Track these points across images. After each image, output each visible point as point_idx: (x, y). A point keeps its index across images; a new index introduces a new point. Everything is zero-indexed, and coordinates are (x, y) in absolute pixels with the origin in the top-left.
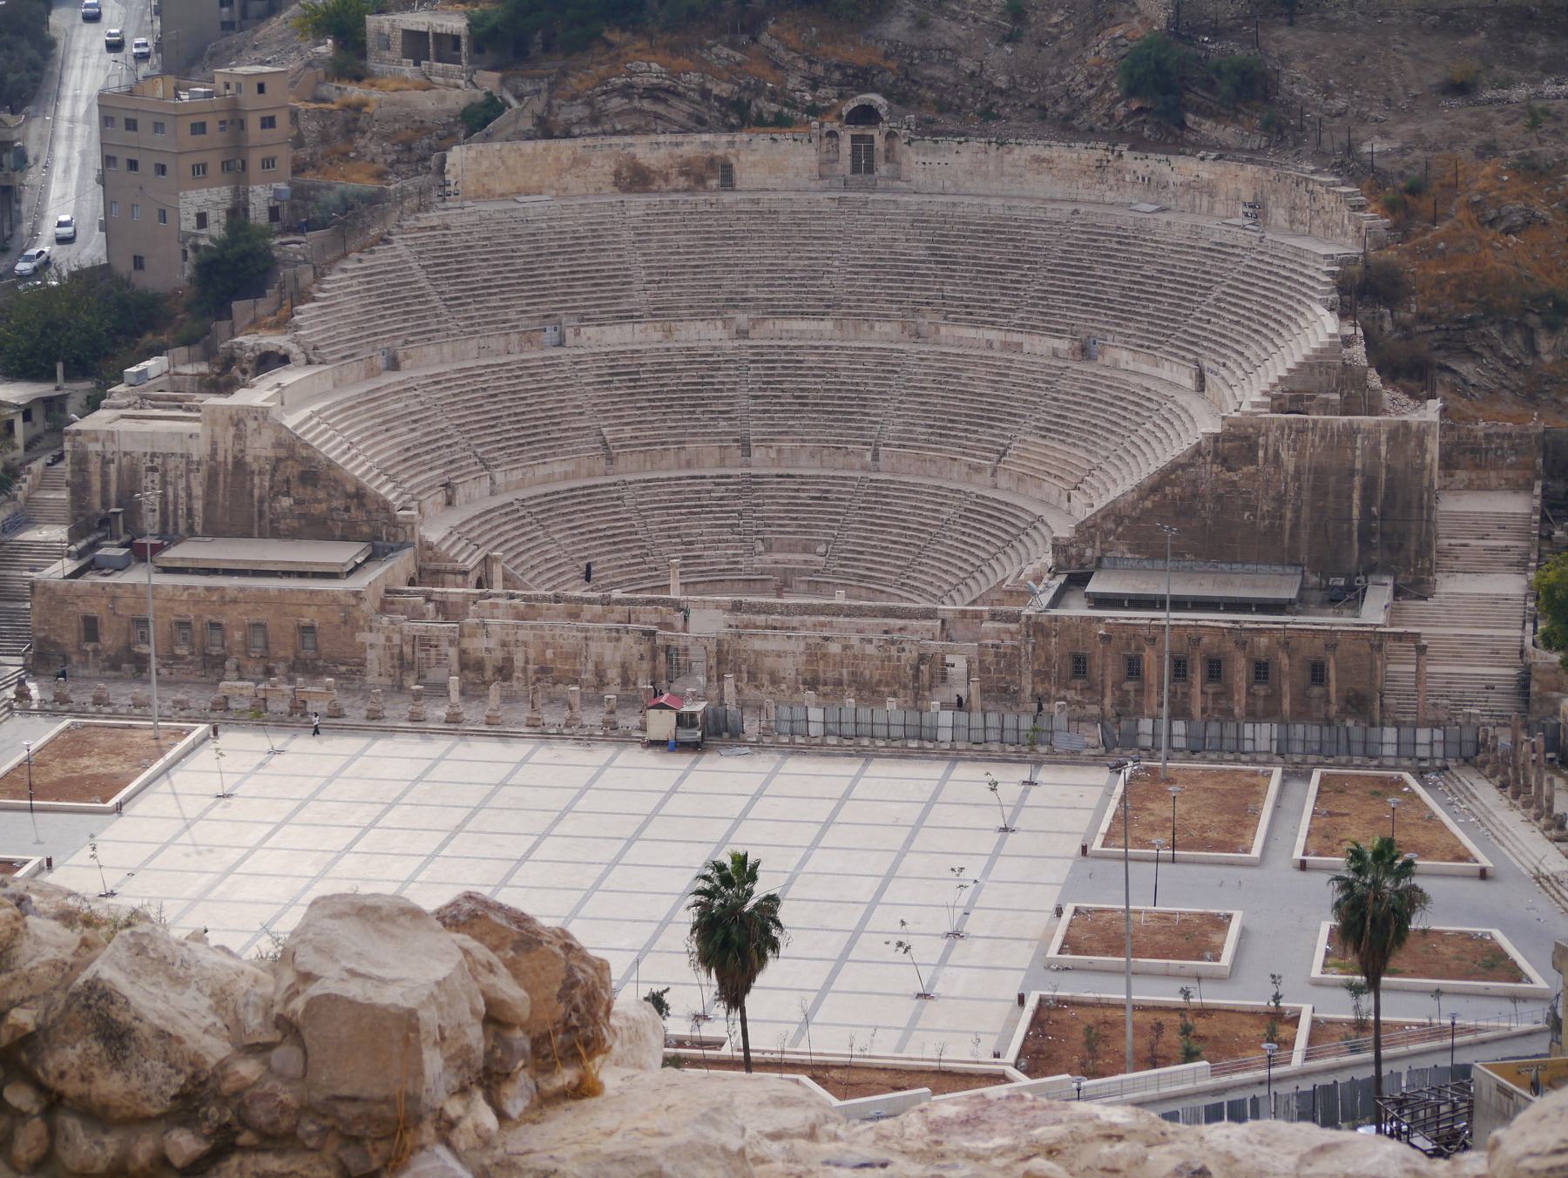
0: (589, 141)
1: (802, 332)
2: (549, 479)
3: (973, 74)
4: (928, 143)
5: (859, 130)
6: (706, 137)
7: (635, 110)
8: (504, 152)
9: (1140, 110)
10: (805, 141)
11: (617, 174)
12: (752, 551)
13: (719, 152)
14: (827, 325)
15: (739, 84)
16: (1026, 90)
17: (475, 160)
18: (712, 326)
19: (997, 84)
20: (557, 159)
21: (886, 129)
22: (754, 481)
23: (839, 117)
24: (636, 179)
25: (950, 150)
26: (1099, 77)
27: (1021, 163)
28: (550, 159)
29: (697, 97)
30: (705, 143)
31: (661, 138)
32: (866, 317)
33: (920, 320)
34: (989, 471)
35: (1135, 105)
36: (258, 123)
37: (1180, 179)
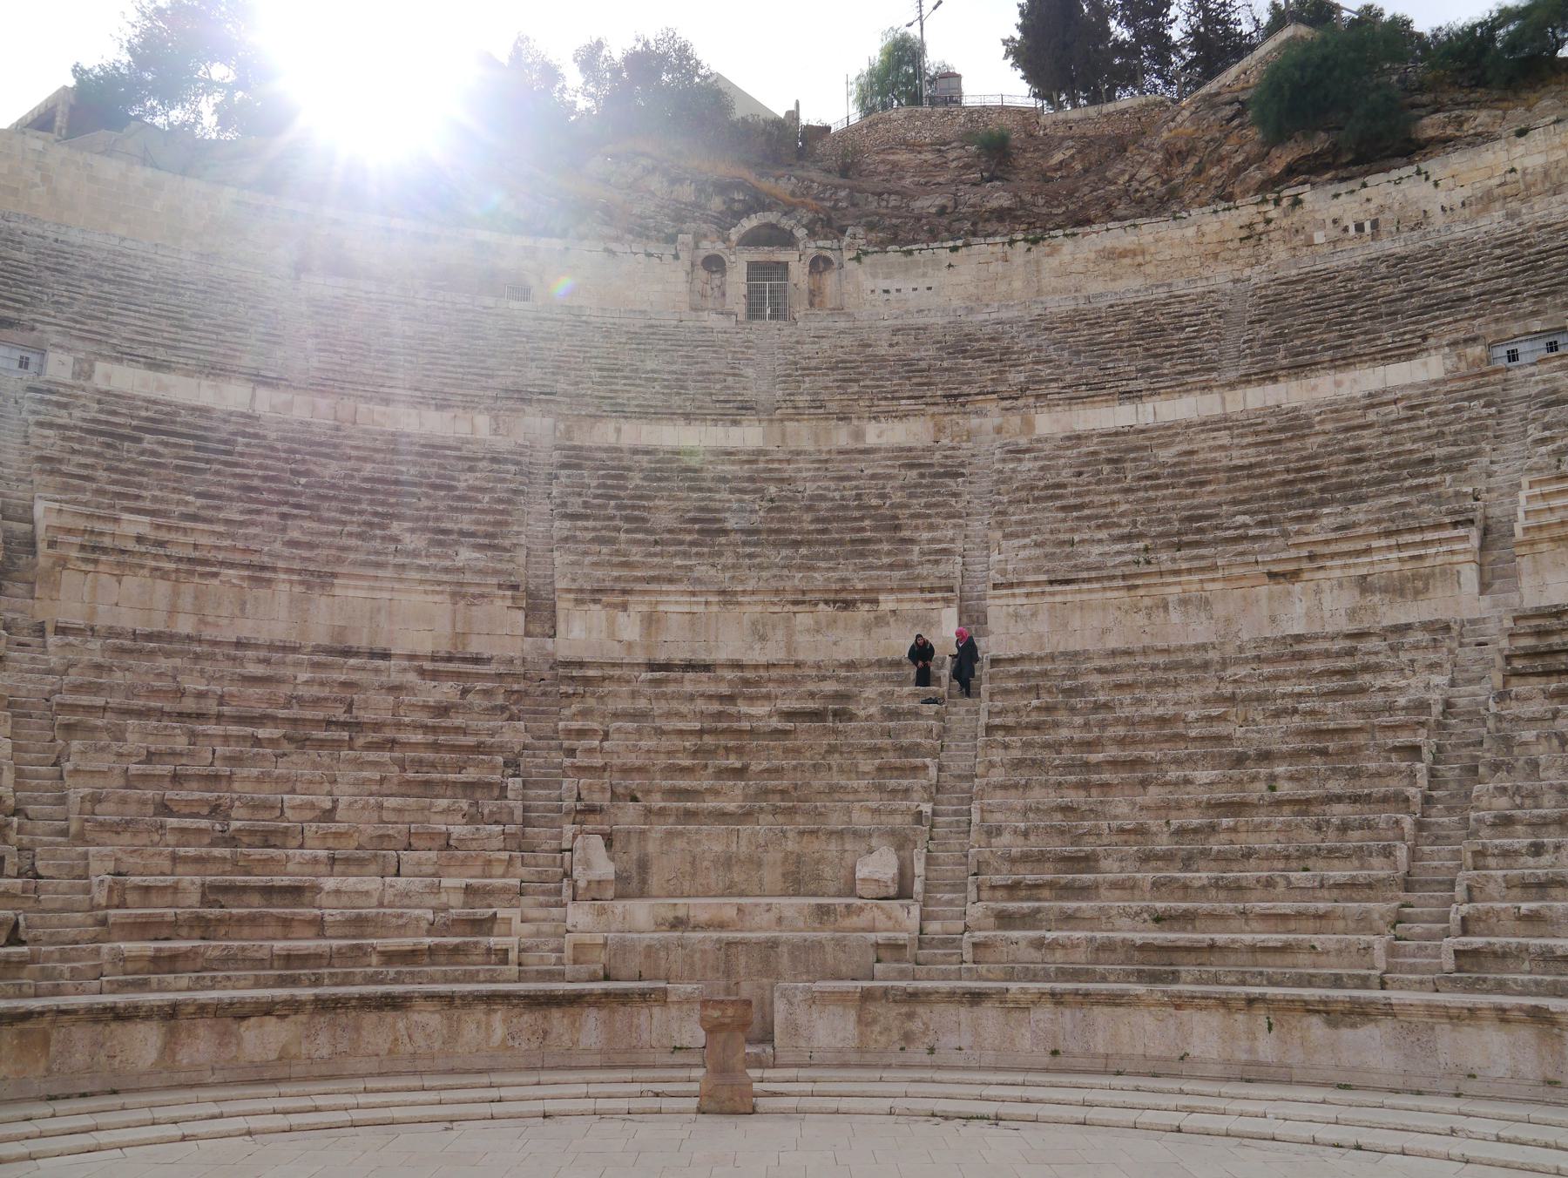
3: (942, 211)
4: (893, 255)
5: (761, 255)
9: (1291, 171)
10: (668, 257)
12: (559, 885)
16: (1044, 210)
19: (994, 204)
21: (812, 251)
22: (575, 677)
23: (726, 240)
25: (936, 263)
26: (1182, 156)
27: (1074, 268)
33: (975, 421)
34: (1470, 575)
35: (1281, 159)
37: (1467, 192)
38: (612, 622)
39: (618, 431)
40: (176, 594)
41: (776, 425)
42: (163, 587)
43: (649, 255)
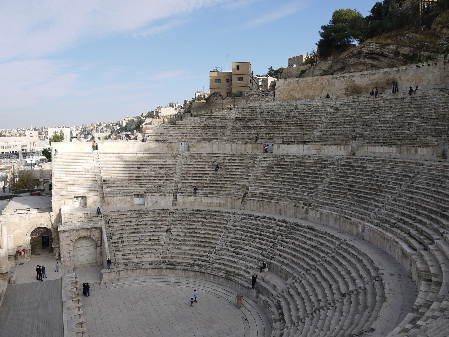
0: (335, 76)
1: (381, 153)
2: (209, 204)
6: (386, 70)
7: (361, 63)
8: (300, 82)
10: (434, 65)
11: (346, 90)
13: (391, 77)
14: (393, 150)
15: (413, 47)
17: (288, 85)
18: (339, 149)
20: (321, 84)
24: (355, 90)
28: (318, 84)
29: (392, 55)
30: (386, 72)
31: (366, 72)
32: (413, 145)
36: (237, 79)
38: (316, 213)
39: (368, 148)
40: (260, 203)
41: (399, 148)
42: (259, 203)
43: (429, 65)
